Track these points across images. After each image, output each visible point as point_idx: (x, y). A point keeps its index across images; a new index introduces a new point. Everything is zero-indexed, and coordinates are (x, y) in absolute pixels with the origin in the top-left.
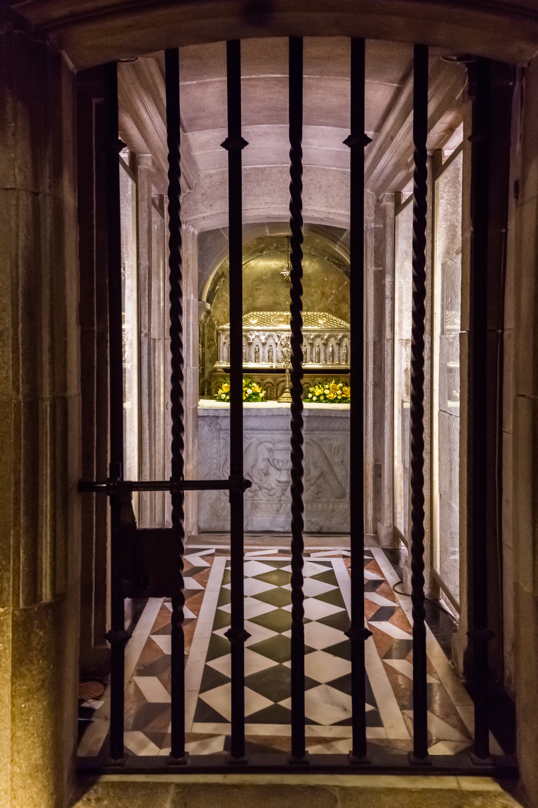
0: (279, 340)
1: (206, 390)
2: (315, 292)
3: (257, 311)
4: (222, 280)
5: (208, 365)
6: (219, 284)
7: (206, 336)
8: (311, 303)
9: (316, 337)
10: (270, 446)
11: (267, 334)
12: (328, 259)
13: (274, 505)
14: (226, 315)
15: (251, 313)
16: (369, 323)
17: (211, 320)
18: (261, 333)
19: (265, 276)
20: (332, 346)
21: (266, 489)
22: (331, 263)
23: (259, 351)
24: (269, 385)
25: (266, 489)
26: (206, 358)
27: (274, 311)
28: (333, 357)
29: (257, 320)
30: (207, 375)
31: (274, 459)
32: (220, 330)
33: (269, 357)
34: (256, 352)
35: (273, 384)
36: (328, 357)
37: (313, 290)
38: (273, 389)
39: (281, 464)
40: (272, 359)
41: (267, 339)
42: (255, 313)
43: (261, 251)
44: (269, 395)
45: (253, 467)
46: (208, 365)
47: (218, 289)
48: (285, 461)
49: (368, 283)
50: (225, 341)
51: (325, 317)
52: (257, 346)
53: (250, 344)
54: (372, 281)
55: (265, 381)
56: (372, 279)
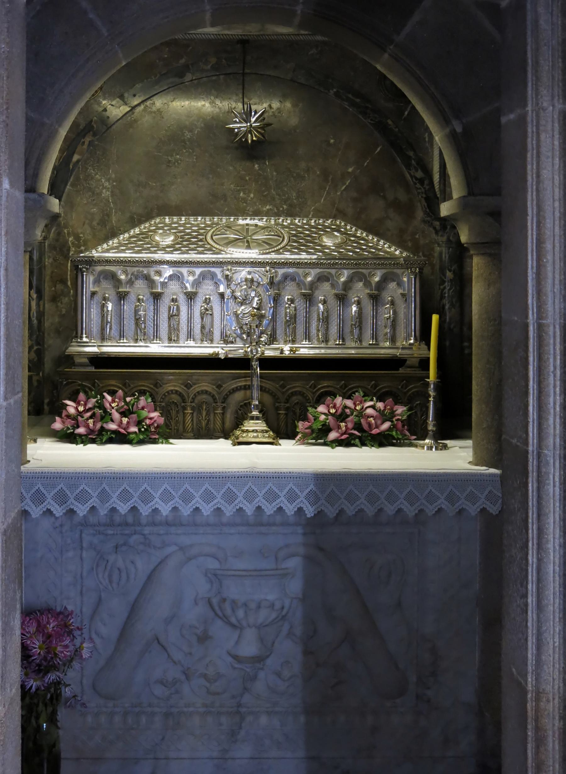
0: (228, 286)
1: (46, 401)
2: (308, 170)
3: (170, 214)
4: (88, 139)
5: (51, 342)
6: (79, 148)
7: (48, 272)
8: (298, 197)
9: (321, 278)
10: (213, 564)
11: (198, 271)
12: (337, 94)
13: (224, 719)
14: (95, 223)
15: (158, 220)
16: (549, 268)
17: (59, 234)
18: (184, 271)
19: (191, 131)
20: (359, 303)
21: (205, 676)
22: (346, 104)
23: (178, 315)
24: (204, 396)
25: (205, 676)
26: (47, 324)
27: (212, 214)
28: (361, 329)
29: (172, 238)
30: (48, 365)
31: (224, 600)
32: (81, 262)
33: (203, 327)
34: (170, 317)
35: (213, 396)
36: (347, 330)
37: (303, 165)
38: (215, 409)
39: (241, 613)
40: (211, 333)
41: (197, 283)
42: (167, 220)
43: (181, 74)
44: (204, 423)
45: (169, 621)
46: (51, 342)
47: (78, 161)
48: (253, 606)
49: (544, 150)
50: (96, 289)
51: (338, 231)
52: (173, 300)
53: (157, 297)
54: (556, 143)
55: (196, 388)
56: (557, 136)
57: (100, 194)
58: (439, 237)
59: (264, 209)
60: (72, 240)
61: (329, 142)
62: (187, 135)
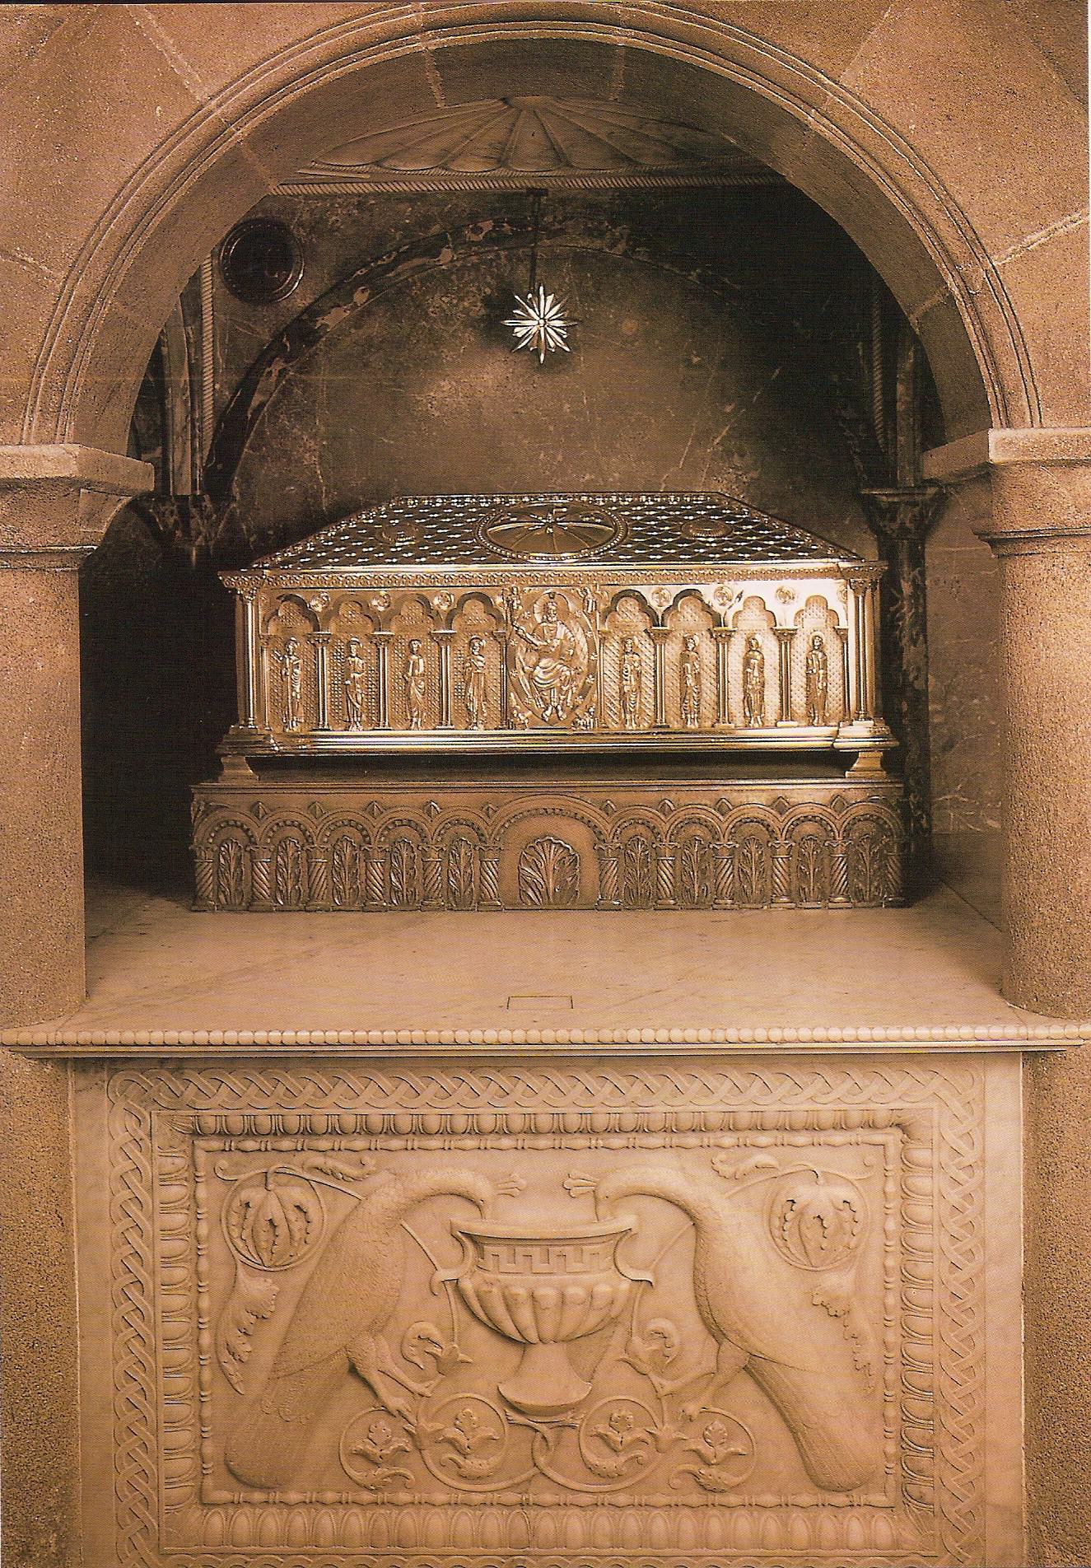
4: (277, 366)
47: (262, 405)
57: (299, 461)
58: (886, 523)
59: (581, 480)
60: (255, 541)
61: (690, 360)
62: (447, 356)
